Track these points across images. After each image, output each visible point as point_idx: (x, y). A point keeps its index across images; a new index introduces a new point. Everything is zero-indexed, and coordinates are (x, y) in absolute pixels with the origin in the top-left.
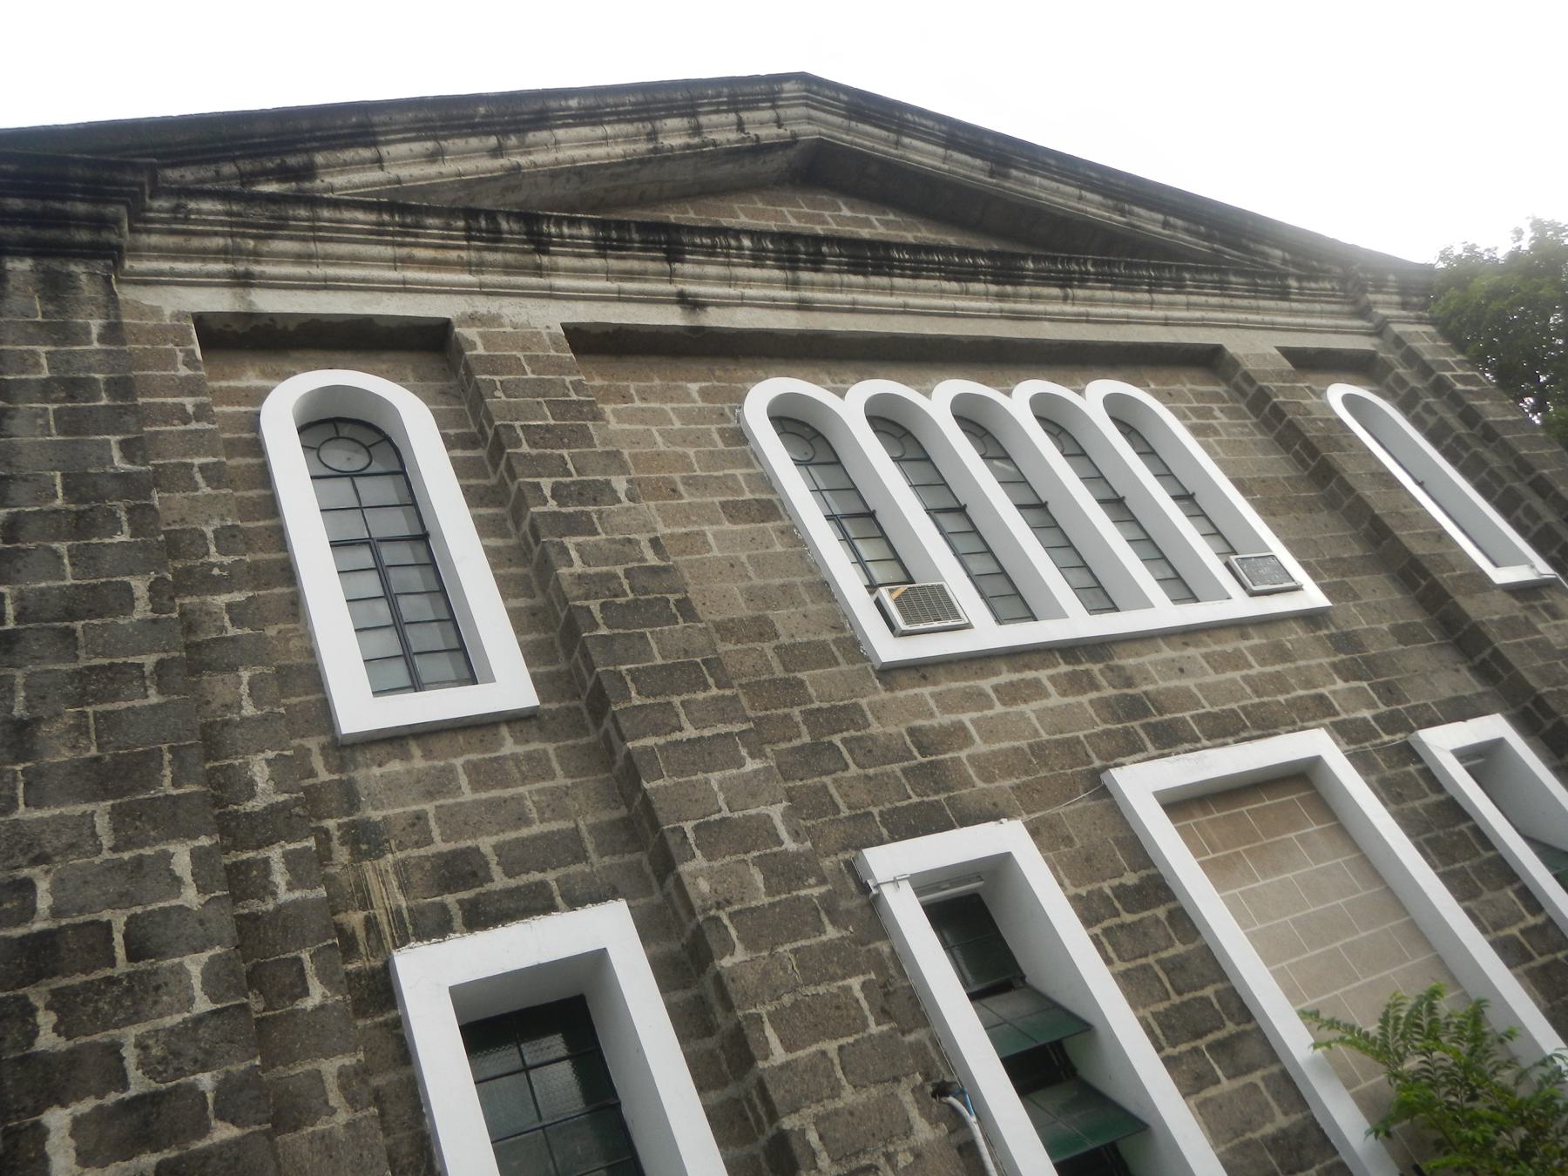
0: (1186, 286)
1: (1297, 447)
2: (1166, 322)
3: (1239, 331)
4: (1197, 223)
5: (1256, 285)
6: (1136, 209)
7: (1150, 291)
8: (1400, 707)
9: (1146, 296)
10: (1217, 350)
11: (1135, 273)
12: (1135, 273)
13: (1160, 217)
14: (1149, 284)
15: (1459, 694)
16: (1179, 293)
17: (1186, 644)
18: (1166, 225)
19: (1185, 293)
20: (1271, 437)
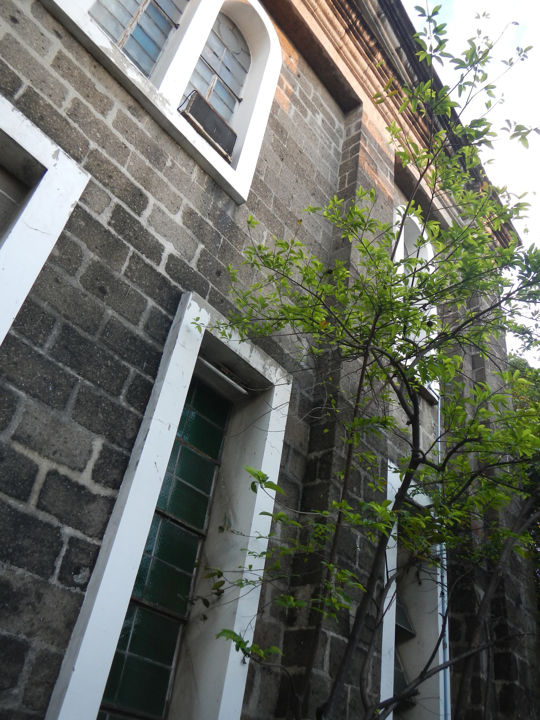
0: (373, 61)
1: (347, 174)
2: (339, 50)
3: (382, 119)
4: (416, 73)
5: (417, 120)
6: (387, 22)
7: (347, 31)
8: (211, 285)
9: (342, 30)
10: (358, 103)
11: (347, 6)
12: (347, 6)
13: (398, 45)
14: (350, 27)
15: (280, 344)
16: (366, 60)
17: (59, 36)
18: (398, 50)
19: (369, 65)
20: (340, 163)
